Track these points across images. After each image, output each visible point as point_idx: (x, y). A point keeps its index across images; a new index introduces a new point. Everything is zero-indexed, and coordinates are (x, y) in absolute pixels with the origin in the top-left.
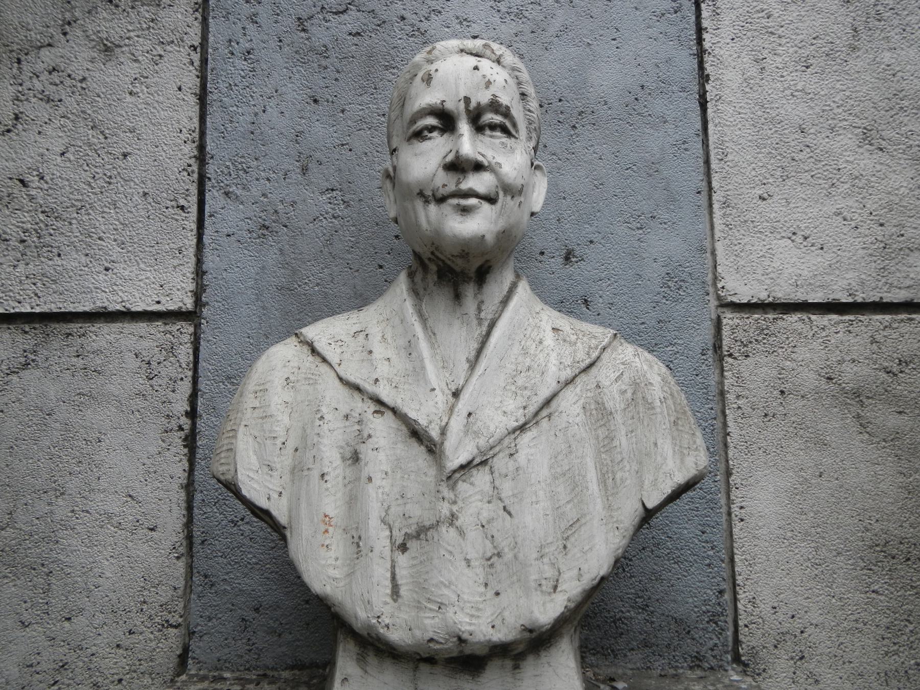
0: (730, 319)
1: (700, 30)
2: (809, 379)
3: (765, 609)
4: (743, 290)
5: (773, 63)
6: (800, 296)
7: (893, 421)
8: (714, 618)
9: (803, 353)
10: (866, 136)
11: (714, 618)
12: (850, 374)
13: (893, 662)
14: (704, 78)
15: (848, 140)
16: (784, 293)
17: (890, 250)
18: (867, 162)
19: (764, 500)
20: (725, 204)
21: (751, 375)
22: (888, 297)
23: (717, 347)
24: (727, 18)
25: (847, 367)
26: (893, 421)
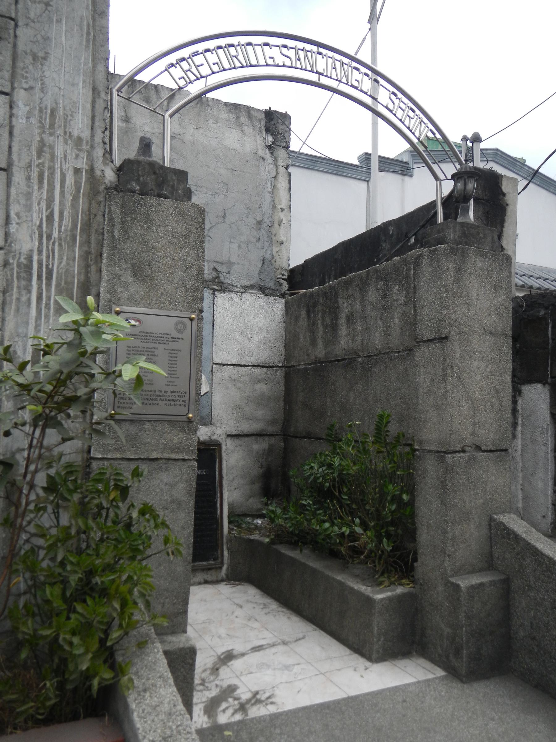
0: (215, 366)
1: (214, 310)
2: (227, 377)
3: (216, 416)
4: (217, 361)
5: (226, 318)
6: (227, 363)
7: (240, 385)
8: (208, 417)
9: (226, 373)
10: (241, 334)
11: (208, 417)
12: (234, 377)
13: (235, 425)
14: (214, 320)
15: (237, 334)
16: (224, 362)
17: (242, 355)
18: (240, 338)
19: (217, 398)
20: (215, 345)
21: (217, 376)
22: (241, 364)
23: (212, 371)
24: (219, 308)
25: (234, 376)
26: (240, 385)
